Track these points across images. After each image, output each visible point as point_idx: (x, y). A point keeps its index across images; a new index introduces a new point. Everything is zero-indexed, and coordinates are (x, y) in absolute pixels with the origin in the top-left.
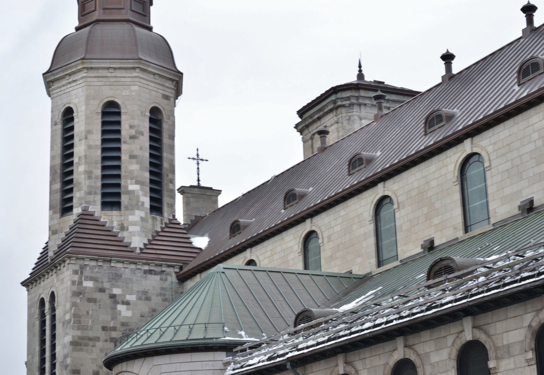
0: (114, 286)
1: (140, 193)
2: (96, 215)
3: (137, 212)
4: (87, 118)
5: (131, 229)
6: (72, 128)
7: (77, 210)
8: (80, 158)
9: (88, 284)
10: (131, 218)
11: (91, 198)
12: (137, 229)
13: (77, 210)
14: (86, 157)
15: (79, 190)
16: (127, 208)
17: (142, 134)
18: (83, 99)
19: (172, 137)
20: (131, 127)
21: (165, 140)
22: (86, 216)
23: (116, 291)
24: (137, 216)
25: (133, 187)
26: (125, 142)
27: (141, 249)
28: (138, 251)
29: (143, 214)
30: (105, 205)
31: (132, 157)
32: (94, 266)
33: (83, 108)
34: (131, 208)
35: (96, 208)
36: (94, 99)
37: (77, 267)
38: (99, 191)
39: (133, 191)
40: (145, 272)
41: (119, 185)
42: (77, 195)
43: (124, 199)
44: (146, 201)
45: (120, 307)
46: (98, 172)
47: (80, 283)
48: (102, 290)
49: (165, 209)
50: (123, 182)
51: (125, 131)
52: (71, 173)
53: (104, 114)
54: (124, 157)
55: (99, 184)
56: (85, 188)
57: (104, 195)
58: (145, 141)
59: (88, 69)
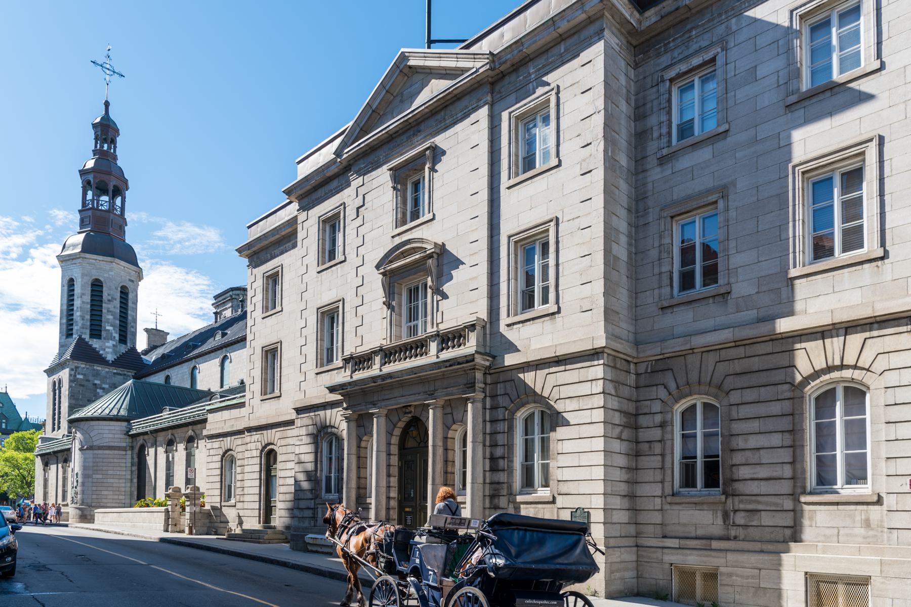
0: (95, 379)
1: (113, 331)
2: (86, 340)
3: (111, 341)
4: (82, 286)
5: (107, 350)
6: (73, 290)
7: (76, 336)
8: (77, 308)
9: (80, 377)
10: (107, 344)
11: (84, 331)
12: (110, 350)
13: (76, 336)
14: (81, 307)
15: (77, 325)
16: (105, 339)
17: (116, 300)
18: (80, 275)
19: (135, 303)
20: (108, 295)
21: (130, 304)
22: (81, 340)
23: (97, 382)
24: (110, 343)
25: (108, 328)
26: (105, 303)
27: (112, 361)
28: (110, 362)
29: (114, 343)
30: (92, 336)
31: (109, 311)
32: (84, 368)
33: (80, 280)
34: (107, 339)
35: (86, 337)
36: (87, 276)
37: (73, 367)
38: (89, 327)
39: (109, 330)
40: (114, 373)
41: (101, 326)
42: (75, 328)
43: (104, 334)
44: (117, 336)
45: (98, 390)
46: (88, 317)
47: (75, 376)
48: (88, 381)
49: (128, 341)
50: (103, 325)
51: (105, 296)
52: (72, 315)
53: (93, 285)
54: (104, 311)
55: (89, 323)
56: (80, 325)
57: (91, 330)
58: (117, 303)
59: (83, 258)
